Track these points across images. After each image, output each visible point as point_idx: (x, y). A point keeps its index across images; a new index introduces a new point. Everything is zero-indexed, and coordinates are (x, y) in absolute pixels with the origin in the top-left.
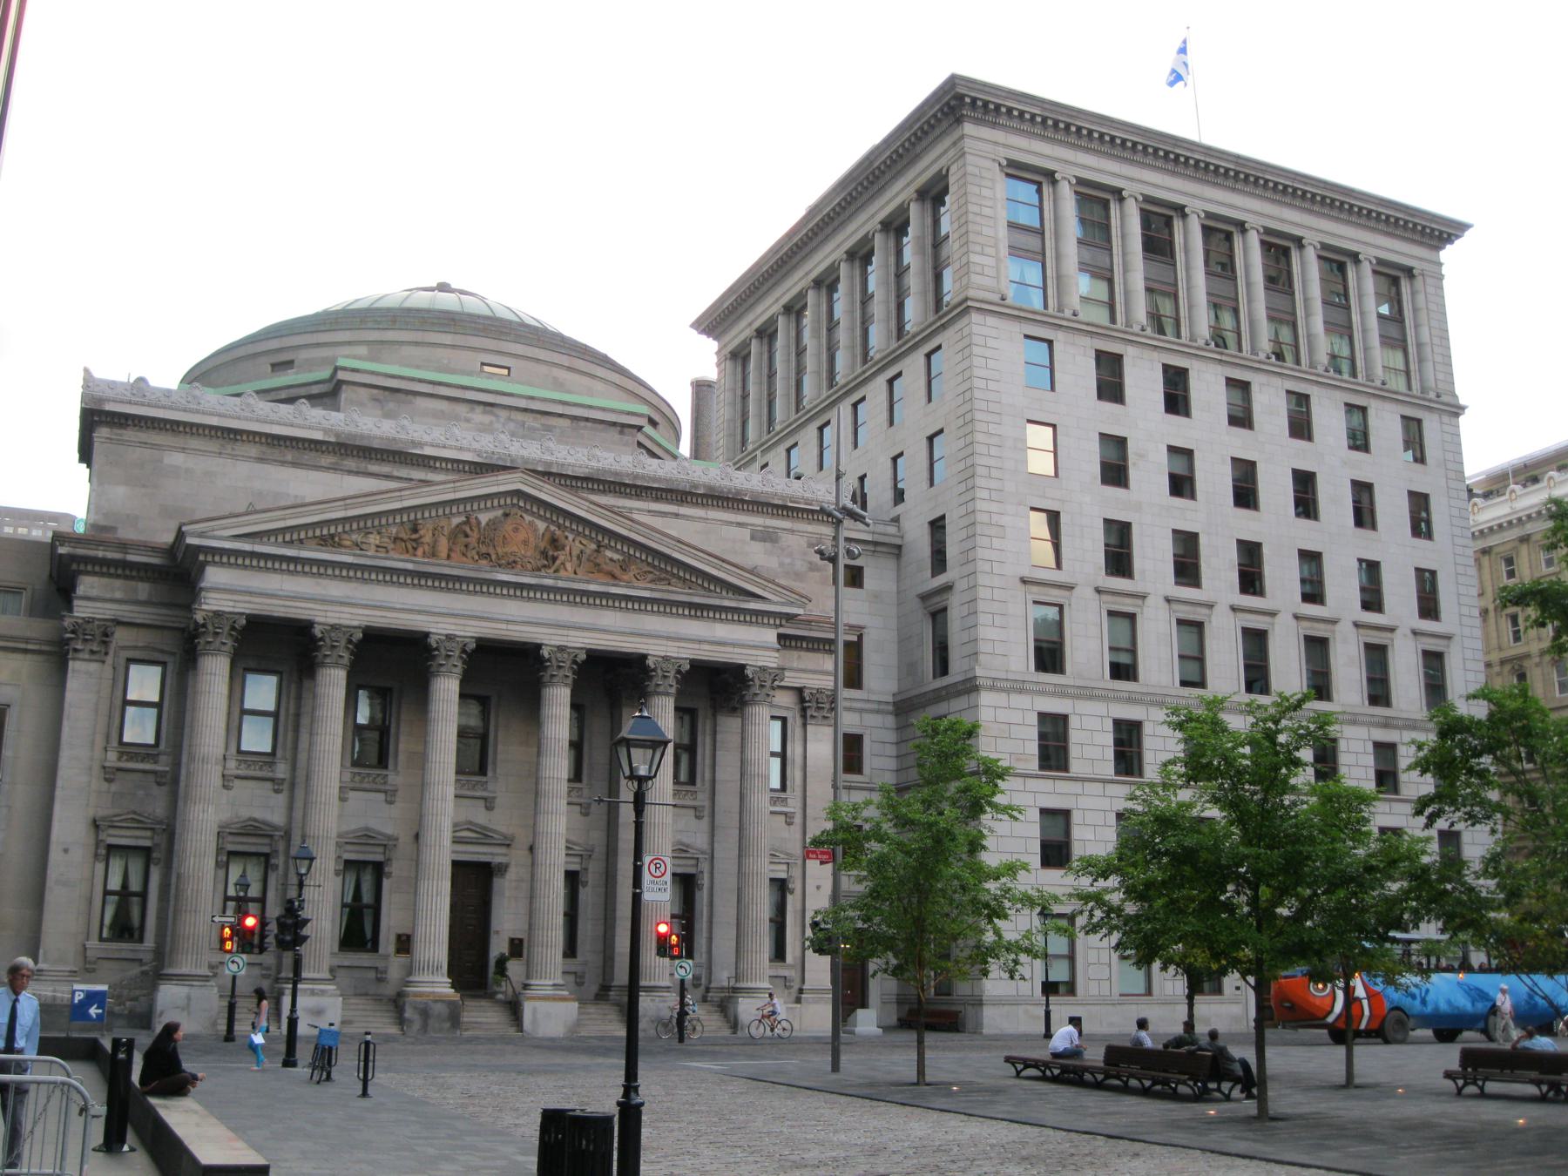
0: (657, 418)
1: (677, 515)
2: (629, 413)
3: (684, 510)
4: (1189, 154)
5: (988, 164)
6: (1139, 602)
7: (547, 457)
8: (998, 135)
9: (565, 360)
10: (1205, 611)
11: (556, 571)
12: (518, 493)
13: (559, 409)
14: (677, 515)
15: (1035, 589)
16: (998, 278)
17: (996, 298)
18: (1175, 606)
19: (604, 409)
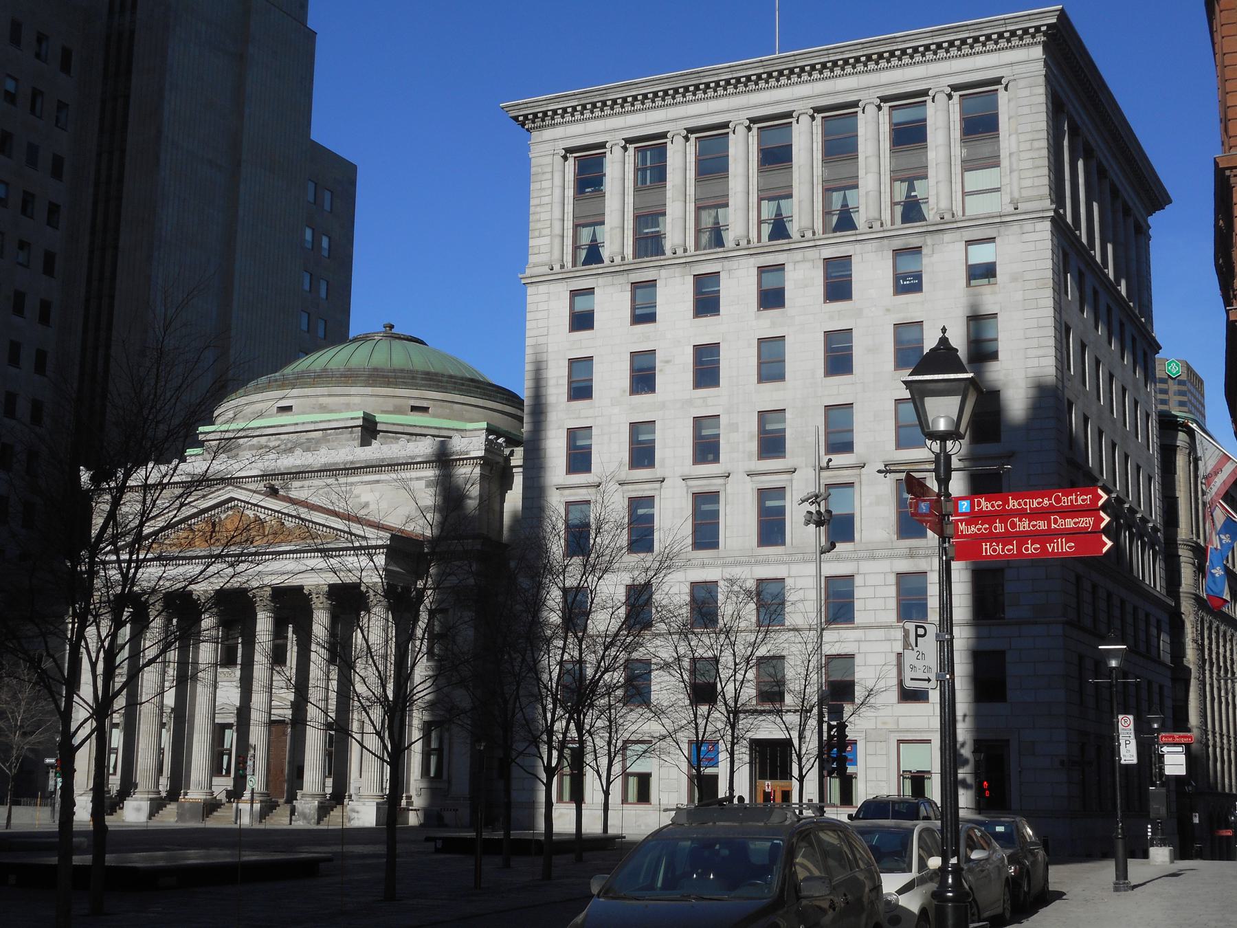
0: (425, 404)
1: (378, 482)
2: (352, 419)
3: (383, 477)
4: (716, 79)
5: (548, 160)
6: (657, 485)
7: (298, 462)
8: (558, 132)
9: (324, 390)
10: (721, 481)
11: (252, 543)
12: (232, 499)
13: (312, 427)
14: (378, 482)
15: (567, 492)
16: (551, 252)
17: (546, 269)
18: (691, 483)
19: (337, 420)
